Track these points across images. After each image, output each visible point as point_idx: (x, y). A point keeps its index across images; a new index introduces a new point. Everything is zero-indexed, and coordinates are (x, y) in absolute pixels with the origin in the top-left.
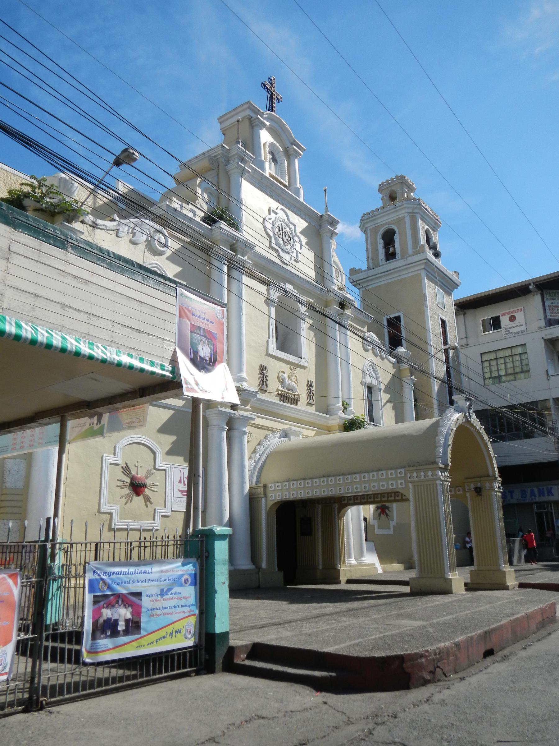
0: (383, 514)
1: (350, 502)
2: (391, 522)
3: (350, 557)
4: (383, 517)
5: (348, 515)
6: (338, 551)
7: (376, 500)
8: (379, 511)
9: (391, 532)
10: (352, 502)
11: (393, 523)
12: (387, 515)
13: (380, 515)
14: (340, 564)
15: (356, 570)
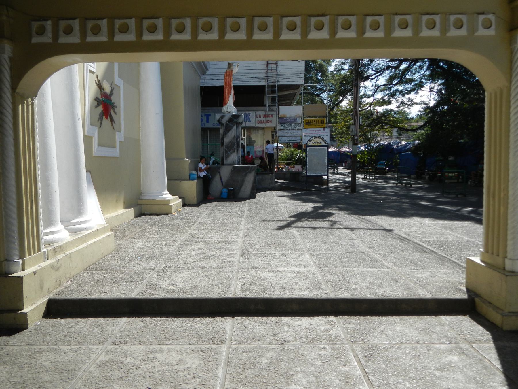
0: (107, 118)
1: (63, 39)
2: (117, 133)
3: (50, 222)
4: (106, 122)
5: (43, 96)
6: (14, 215)
7: (175, 37)
8: (101, 108)
9: (116, 152)
10: (75, 39)
11: (119, 137)
12: (112, 121)
13: (101, 119)
14: (22, 257)
15: (70, 256)
